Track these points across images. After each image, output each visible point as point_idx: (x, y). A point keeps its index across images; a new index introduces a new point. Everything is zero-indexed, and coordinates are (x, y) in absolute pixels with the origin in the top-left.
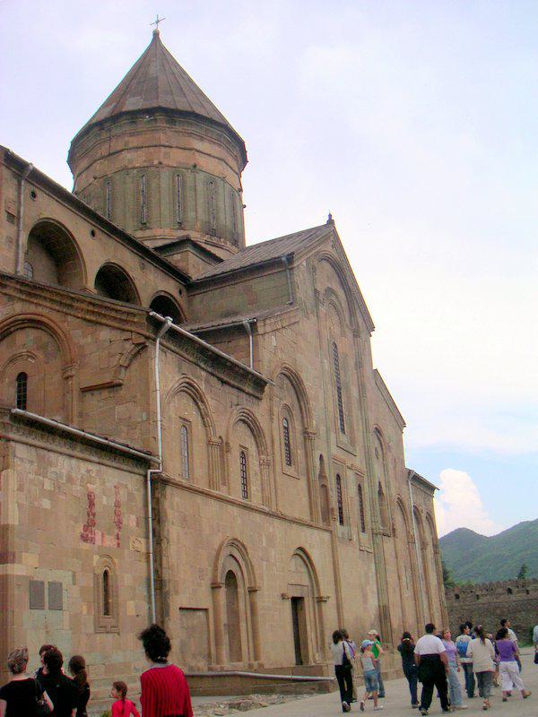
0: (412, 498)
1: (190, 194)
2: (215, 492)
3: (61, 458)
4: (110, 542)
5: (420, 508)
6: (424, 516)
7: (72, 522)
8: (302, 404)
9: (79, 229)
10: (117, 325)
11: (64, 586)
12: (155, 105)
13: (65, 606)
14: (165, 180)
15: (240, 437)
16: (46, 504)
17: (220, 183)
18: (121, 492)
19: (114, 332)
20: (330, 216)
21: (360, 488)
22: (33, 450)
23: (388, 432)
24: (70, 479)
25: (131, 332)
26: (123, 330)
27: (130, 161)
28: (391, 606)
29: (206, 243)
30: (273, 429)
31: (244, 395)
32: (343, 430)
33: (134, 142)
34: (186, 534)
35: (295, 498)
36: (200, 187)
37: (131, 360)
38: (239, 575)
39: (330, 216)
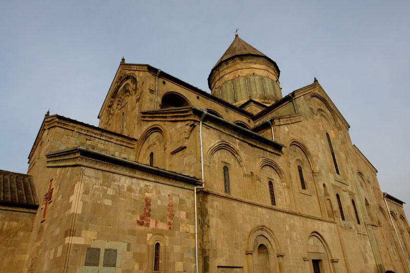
0: (388, 206)
1: (252, 85)
3: (123, 178)
5: (395, 213)
6: (398, 216)
7: (129, 214)
8: (309, 159)
10: (182, 119)
11: (118, 252)
12: (234, 55)
13: (118, 265)
14: (242, 81)
18: (174, 198)
20: (315, 79)
21: (353, 202)
22: (100, 172)
23: (367, 174)
24: (130, 189)
25: (188, 120)
26: (185, 121)
28: (384, 265)
31: (268, 153)
33: (228, 71)
34: (223, 222)
36: (257, 81)
37: (190, 135)
39: (315, 79)
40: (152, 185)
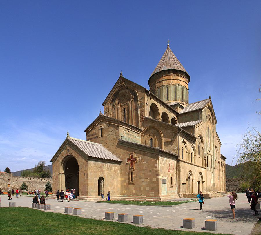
1: (178, 91)
2: (188, 162)
4: (172, 172)
9: (158, 105)
15: (192, 150)
16: (164, 166)
17: (184, 88)
19: (171, 131)
24: (167, 161)
27: (164, 83)
29: (181, 104)
30: (196, 147)
32: (209, 147)
33: (165, 78)
35: (200, 162)
37: (174, 137)
38: (190, 177)
40: (170, 159)
